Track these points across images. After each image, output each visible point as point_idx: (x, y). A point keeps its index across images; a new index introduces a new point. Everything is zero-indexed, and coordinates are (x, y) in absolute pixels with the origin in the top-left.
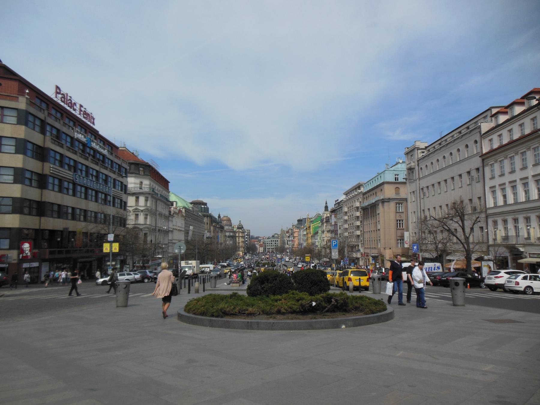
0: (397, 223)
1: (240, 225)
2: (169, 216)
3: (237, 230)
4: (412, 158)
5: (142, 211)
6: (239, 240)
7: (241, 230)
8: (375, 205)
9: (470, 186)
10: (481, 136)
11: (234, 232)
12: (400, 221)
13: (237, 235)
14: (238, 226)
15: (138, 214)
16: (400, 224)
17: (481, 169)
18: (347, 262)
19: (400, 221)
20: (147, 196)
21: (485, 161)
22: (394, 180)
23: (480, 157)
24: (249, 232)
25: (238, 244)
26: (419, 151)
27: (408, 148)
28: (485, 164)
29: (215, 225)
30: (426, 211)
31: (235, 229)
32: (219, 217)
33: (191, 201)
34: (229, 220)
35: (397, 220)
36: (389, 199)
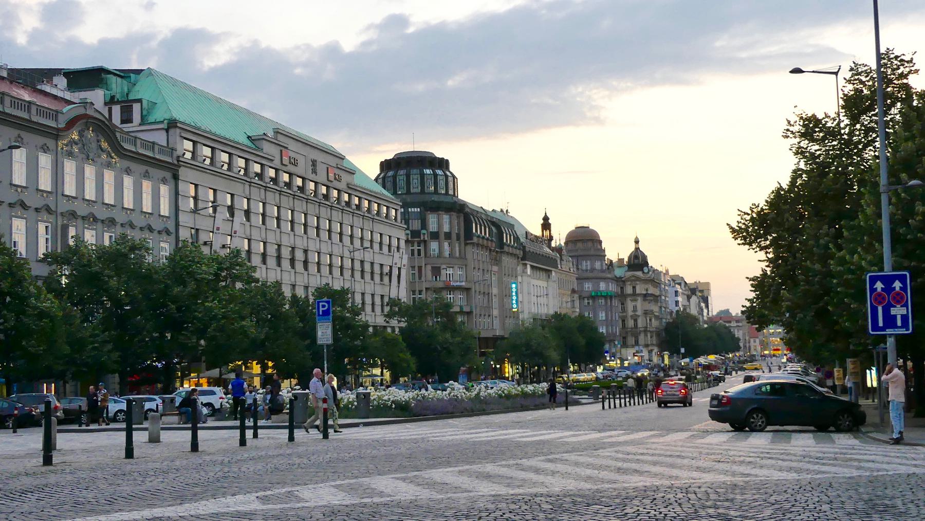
3: (630, 273)
7: (639, 274)
11: (620, 281)
13: (629, 290)
14: (630, 258)
18: (898, 311)
24: (709, 290)
31: (618, 272)
32: (546, 225)
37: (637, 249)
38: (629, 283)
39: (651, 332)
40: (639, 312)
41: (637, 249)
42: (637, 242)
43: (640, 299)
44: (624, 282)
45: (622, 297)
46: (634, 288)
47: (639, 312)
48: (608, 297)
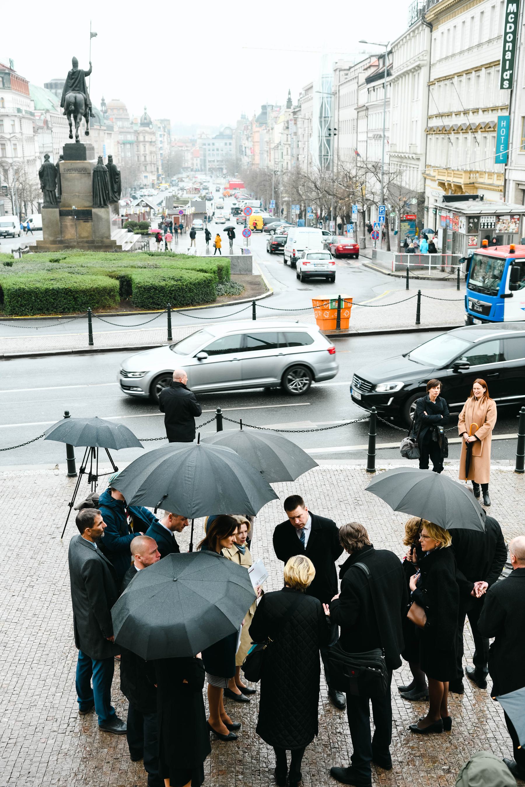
1: (145, 119)
2: (34, 136)
3: (142, 129)
5: (9, 140)
6: (145, 151)
7: (147, 129)
11: (137, 133)
13: (141, 138)
14: (141, 120)
15: (4, 144)
20: (13, 118)
21: (360, 113)
25: (142, 159)
26: (342, 73)
29: (98, 128)
33: (48, 81)
34: (123, 109)
37: (145, 113)
38: (141, 134)
39: (154, 164)
40: (147, 152)
41: (145, 113)
42: (145, 109)
43: (148, 145)
44: (138, 133)
45: (138, 142)
46: (144, 137)
47: (147, 152)
48: (131, 143)
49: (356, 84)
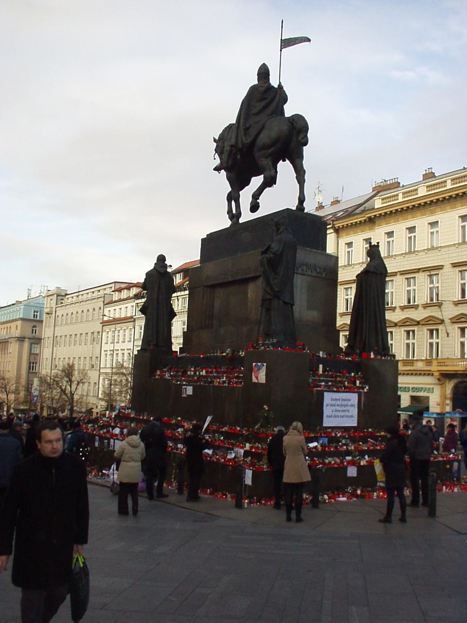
0: (30, 366)
4: (52, 302)
8: (8, 341)
9: (92, 345)
10: (104, 305)
12: (33, 364)
16: (33, 366)
17: (101, 333)
19: (33, 364)
22: (32, 317)
23: (100, 323)
26: (60, 298)
27: (49, 291)
28: (104, 329)
30: (57, 359)
35: (30, 363)
36: (24, 338)
49: (102, 302)
